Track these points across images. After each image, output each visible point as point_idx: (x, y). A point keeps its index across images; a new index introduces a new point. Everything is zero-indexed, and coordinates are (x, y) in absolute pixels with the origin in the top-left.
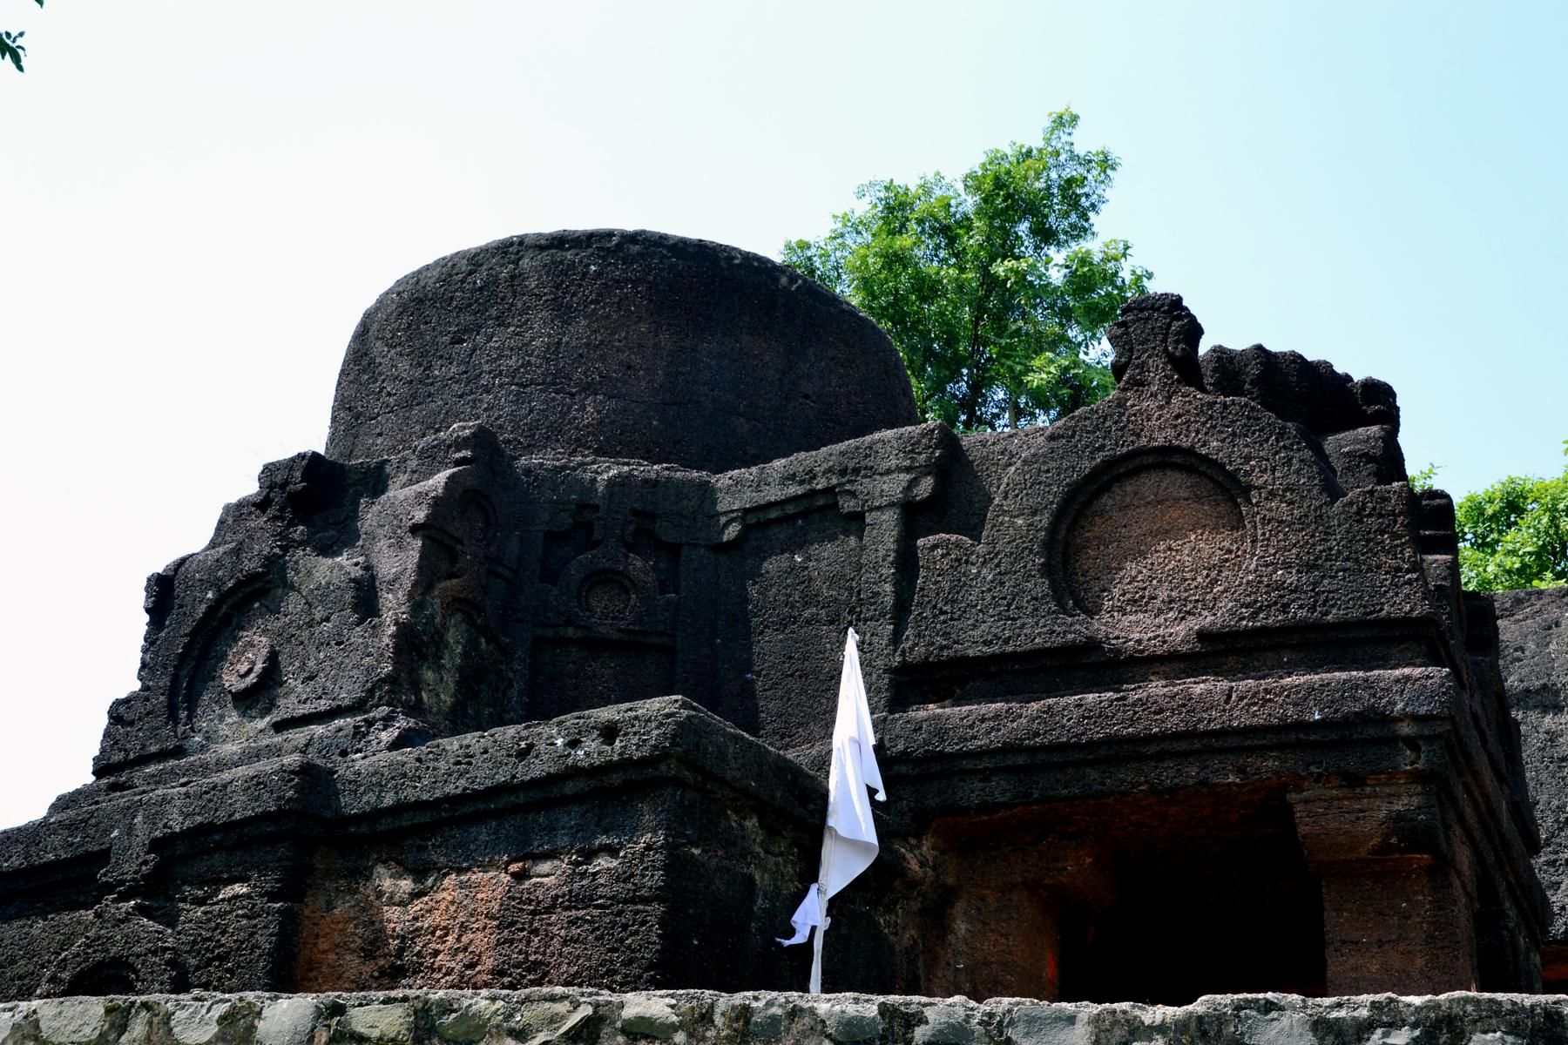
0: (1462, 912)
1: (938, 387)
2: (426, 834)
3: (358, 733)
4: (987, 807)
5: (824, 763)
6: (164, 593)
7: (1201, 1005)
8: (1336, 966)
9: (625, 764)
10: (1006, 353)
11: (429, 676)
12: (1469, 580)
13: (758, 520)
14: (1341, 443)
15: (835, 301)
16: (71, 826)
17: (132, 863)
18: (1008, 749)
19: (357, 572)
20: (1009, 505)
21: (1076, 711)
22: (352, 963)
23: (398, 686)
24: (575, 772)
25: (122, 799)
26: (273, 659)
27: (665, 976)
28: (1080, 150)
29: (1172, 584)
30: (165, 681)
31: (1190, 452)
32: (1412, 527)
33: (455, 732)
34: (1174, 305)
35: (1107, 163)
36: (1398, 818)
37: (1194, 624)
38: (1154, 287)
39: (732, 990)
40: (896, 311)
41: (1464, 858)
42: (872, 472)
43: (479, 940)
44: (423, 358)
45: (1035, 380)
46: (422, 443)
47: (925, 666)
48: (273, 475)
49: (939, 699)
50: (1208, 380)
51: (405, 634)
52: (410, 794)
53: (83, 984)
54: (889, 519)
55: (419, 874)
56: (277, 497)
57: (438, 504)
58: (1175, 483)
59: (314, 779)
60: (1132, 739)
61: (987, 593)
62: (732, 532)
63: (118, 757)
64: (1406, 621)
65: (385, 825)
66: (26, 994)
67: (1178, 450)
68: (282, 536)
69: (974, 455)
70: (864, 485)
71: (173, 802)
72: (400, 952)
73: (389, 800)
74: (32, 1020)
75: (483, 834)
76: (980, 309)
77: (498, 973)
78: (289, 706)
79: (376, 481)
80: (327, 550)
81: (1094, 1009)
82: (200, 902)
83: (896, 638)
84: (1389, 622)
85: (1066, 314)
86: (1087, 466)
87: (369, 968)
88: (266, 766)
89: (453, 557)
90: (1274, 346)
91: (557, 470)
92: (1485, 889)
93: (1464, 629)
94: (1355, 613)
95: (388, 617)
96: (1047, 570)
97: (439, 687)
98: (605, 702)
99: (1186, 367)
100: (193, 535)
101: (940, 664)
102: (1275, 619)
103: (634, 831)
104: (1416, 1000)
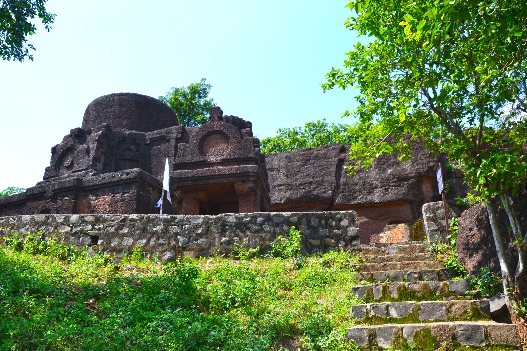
0: (258, 201)
1: (183, 120)
2: (98, 189)
3: (86, 173)
4: (189, 186)
5: (162, 179)
6: (54, 150)
7: (219, 215)
8: (240, 210)
9: (130, 179)
10: (193, 115)
11: (98, 164)
12: (262, 152)
13: (153, 140)
14: (244, 131)
15: (166, 105)
16: (39, 187)
17: (50, 194)
18: (192, 177)
19: (86, 147)
20: (193, 139)
21: (203, 171)
22: (86, 210)
23: (93, 166)
24: (122, 180)
25: (48, 183)
26: (72, 161)
27: (136, 212)
28: (206, 84)
29: (217, 152)
30: (54, 165)
31: (221, 131)
32: (253, 144)
33: (103, 173)
34: (219, 108)
35: (210, 86)
36: (250, 187)
37: (221, 158)
38: (217, 106)
39: (147, 214)
40: (176, 107)
41: (259, 193)
42: (171, 133)
43: (107, 206)
44: (98, 113)
45: (198, 119)
46: (97, 127)
47: (179, 164)
48: (72, 131)
49: (181, 169)
50: (224, 120)
51: (94, 157)
52: (95, 183)
53: (42, 212)
54: (174, 140)
55: (96, 196)
56: (73, 135)
57: (100, 137)
58: (219, 136)
59: (79, 180)
60: (211, 176)
61: (189, 152)
62: (148, 142)
63: (47, 177)
64: (252, 158)
65: (91, 188)
66: (33, 214)
67: (219, 131)
68: (74, 141)
69: (188, 131)
70: (170, 135)
71: (56, 183)
72: (94, 208)
73: (91, 184)
74: (33, 218)
75: (107, 190)
76: (190, 108)
77: (110, 212)
78: (75, 169)
79: (90, 132)
80: (81, 144)
81: (204, 216)
82: (61, 200)
83: (174, 160)
84: (249, 158)
85: (203, 109)
86: (205, 133)
87: (88, 211)
88: (71, 178)
89: (102, 145)
90: (234, 115)
91: (120, 131)
92: (262, 198)
93: (261, 159)
94: (245, 157)
95: (91, 155)
96: (198, 149)
97: (100, 166)
98: (127, 169)
99: (221, 118)
100: (59, 140)
101: (181, 164)
102: (233, 157)
103: (132, 190)
104: (250, 214)
